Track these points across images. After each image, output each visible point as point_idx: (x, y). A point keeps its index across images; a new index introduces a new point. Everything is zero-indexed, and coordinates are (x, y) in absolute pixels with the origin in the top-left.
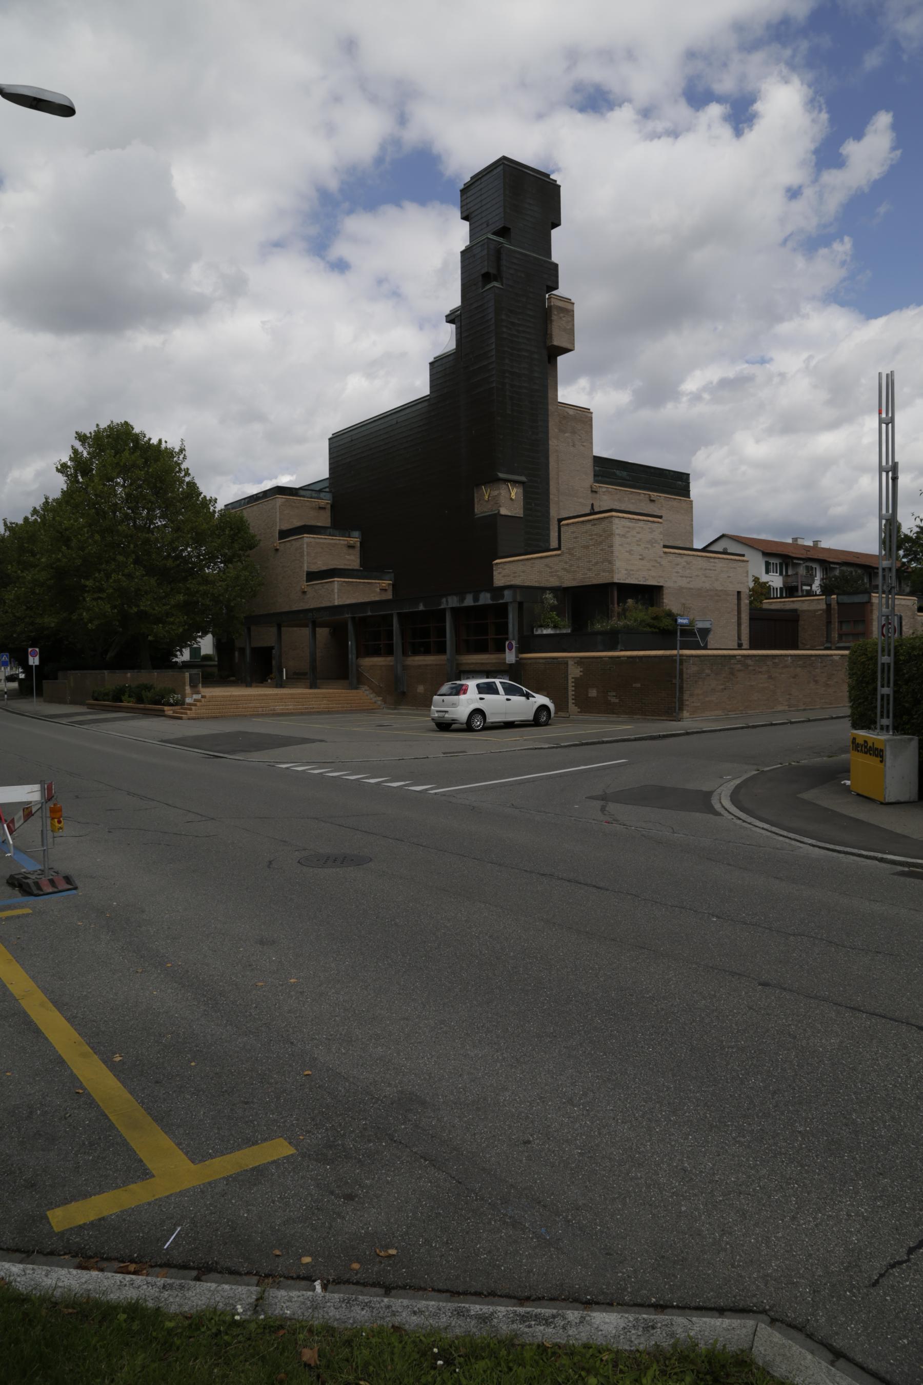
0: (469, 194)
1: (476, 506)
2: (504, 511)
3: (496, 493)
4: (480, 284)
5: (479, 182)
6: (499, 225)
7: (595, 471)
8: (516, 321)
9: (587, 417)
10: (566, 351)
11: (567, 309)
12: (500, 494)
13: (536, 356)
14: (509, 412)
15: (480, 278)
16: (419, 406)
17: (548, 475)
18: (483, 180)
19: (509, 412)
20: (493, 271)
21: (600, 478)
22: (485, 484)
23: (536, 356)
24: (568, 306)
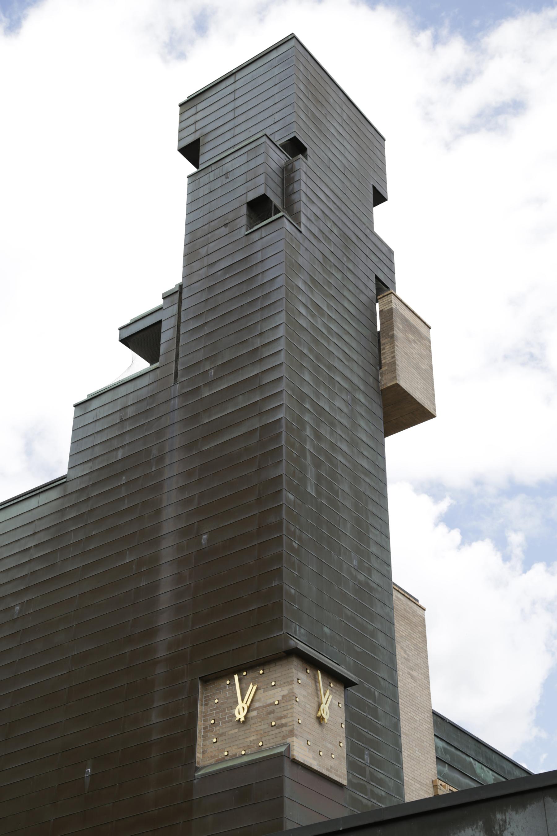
0: (200, 107)
1: (200, 741)
2: (301, 753)
3: (275, 696)
4: (243, 221)
5: (231, 80)
6: (281, 138)
7: (437, 748)
8: (325, 308)
9: (414, 614)
10: (419, 413)
11: (420, 331)
12: (290, 697)
13: (361, 397)
14: (311, 490)
15: (244, 210)
16: (33, 503)
17: (396, 686)
18: (238, 76)
19: (311, 490)
20: (276, 201)
21: (446, 769)
22: (239, 671)
23: (361, 397)
24: (422, 329)
